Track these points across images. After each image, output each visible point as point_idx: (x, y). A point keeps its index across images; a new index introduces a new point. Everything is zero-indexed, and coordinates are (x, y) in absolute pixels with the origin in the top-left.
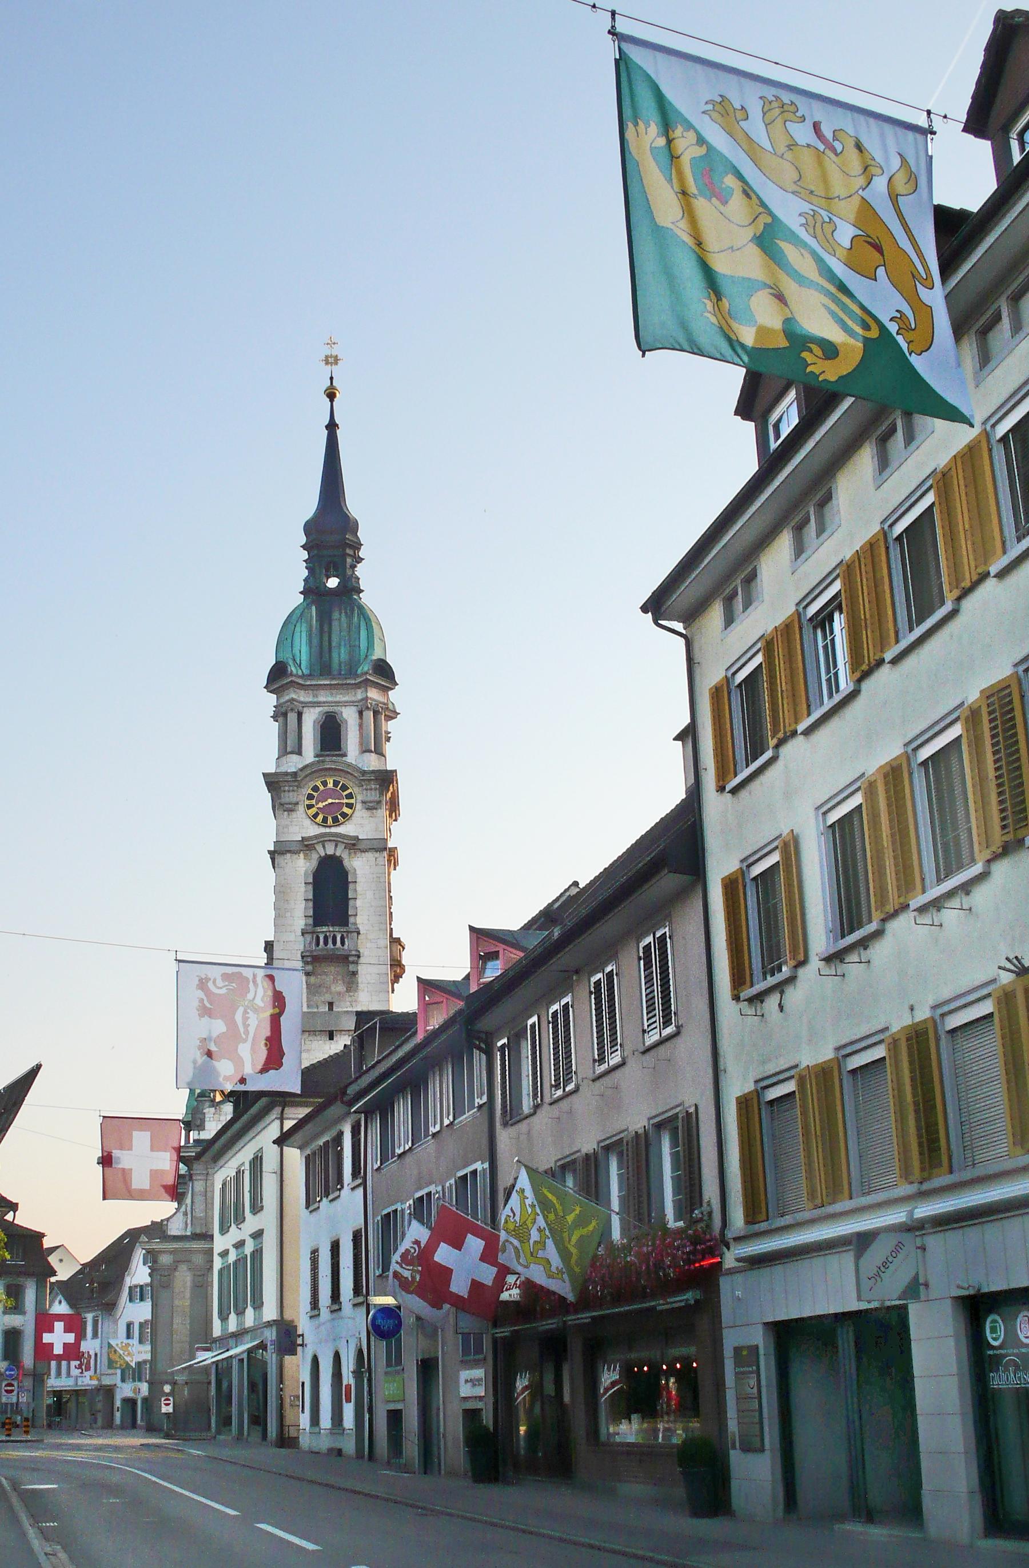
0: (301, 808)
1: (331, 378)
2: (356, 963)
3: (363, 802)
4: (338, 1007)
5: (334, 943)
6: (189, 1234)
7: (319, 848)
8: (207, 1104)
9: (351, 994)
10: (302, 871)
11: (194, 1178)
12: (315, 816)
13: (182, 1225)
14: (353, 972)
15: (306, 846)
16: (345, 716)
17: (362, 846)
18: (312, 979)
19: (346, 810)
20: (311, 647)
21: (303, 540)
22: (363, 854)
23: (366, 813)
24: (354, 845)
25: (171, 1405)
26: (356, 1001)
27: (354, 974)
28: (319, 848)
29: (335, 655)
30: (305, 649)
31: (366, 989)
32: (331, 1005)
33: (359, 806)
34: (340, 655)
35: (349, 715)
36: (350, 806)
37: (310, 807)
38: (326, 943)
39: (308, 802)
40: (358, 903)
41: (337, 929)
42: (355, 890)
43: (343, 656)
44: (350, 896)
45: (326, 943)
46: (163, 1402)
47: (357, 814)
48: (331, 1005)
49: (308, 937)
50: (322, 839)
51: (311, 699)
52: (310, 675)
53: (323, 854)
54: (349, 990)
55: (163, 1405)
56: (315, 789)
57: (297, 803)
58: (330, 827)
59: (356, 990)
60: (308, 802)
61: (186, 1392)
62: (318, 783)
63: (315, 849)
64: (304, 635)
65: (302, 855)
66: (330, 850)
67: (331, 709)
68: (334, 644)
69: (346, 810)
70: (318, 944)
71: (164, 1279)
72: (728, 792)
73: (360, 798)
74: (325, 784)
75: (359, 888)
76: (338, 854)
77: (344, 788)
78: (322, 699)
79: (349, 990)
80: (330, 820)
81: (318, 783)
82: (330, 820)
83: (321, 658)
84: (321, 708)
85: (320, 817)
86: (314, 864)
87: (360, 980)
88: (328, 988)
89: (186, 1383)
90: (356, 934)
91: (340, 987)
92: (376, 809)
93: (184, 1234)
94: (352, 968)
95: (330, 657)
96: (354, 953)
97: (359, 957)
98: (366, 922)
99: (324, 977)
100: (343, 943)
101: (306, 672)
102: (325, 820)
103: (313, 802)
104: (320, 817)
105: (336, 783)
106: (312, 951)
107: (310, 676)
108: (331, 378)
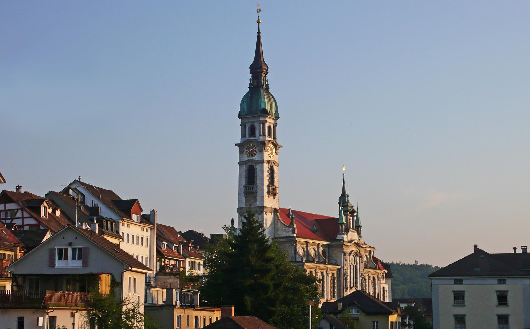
0: (245, 152)
1: (259, 17)
2: (256, 194)
3: (259, 150)
5: (250, 189)
7: (248, 163)
12: (248, 154)
16: (256, 125)
18: (247, 199)
19: (255, 152)
21: (250, 71)
23: (259, 153)
27: (256, 197)
28: (248, 163)
30: (246, 106)
32: (251, 205)
35: (257, 125)
36: (255, 151)
37: (246, 152)
40: (257, 178)
41: (251, 185)
42: (256, 174)
44: (255, 176)
47: (257, 153)
50: (248, 161)
51: (248, 121)
52: (247, 114)
53: (249, 165)
56: (248, 147)
57: (244, 151)
58: (251, 157)
59: (256, 201)
60: (246, 151)
62: (249, 146)
63: (247, 164)
65: (245, 165)
66: (251, 164)
67: (253, 123)
69: (255, 152)
70: (247, 190)
72: (71, 248)
73: (258, 149)
74: (250, 145)
76: (252, 165)
77: (254, 146)
78: (250, 121)
80: (251, 155)
81: (249, 146)
82: (251, 155)
85: (249, 155)
86: (247, 167)
90: (256, 187)
94: (255, 195)
97: (257, 192)
98: (259, 183)
100: (252, 189)
101: (246, 113)
102: (250, 155)
103: (247, 150)
104: (249, 155)
105: (252, 145)
107: (247, 114)
108: (259, 17)
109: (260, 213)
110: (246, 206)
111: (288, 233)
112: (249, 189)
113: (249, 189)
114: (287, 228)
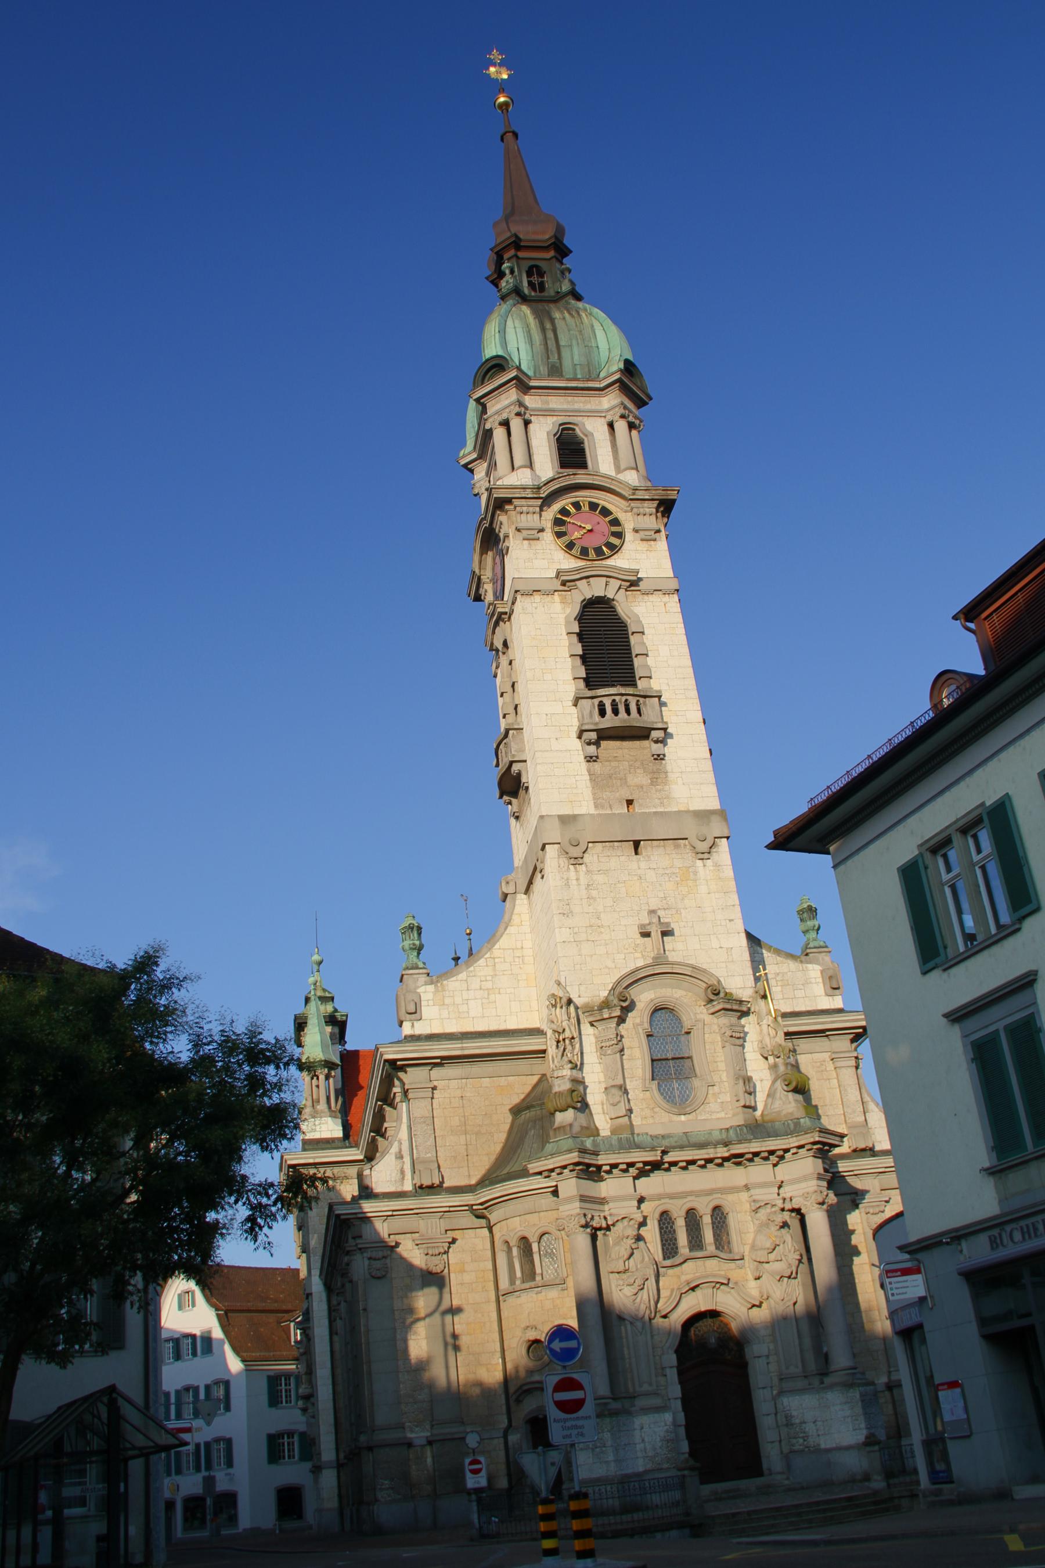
4: (641, 805)
5: (628, 711)
6: (408, 1187)
8: (423, 979)
9: (658, 787)
10: (561, 619)
11: (410, 1096)
13: (396, 1175)
14: (659, 755)
15: (564, 583)
17: (643, 585)
18: (597, 766)
20: (532, 345)
22: (645, 597)
24: (631, 585)
25: (483, 1473)
26: (668, 797)
27: (659, 757)
29: (566, 354)
31: (680, 781)
33: (629, 536)
34: (572, 357)
38: (616, 712)
39: (557, 529)
43: (576, 358)
45: (616, 712)
46: (467, 1468)
48: (630, 802)
49: (586, 704)
54: (654, 782)
55: (468, 1475)
59: (666, 781)
61: (429, 1460)
64: (519, 330)
68: (562, 343)
71: (377, 1264)
75: (648, 639)
76: (610, 595)
79: (654, 782)
83: (548, 358)
84: (555, 418)
87: (669, 768)
88: (624, 780)
89: (430, 1443)
91: (640, 778)
92: (655, 540)
93: (399, 1190)
95: (560, 357)
96: (660, 726)
99: (613, 764)
106: (596, 724)
109: (703, 847)
110: (596, 807)
111: (799, 993)
112: (622, 708)
113: (622, 708)
114: (792, 965)
